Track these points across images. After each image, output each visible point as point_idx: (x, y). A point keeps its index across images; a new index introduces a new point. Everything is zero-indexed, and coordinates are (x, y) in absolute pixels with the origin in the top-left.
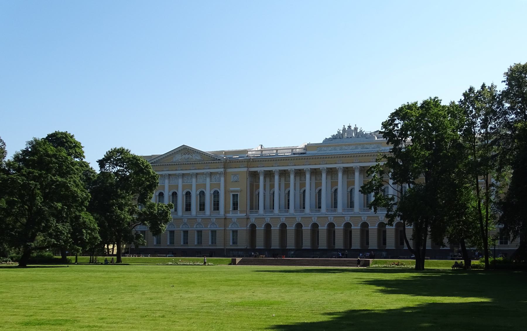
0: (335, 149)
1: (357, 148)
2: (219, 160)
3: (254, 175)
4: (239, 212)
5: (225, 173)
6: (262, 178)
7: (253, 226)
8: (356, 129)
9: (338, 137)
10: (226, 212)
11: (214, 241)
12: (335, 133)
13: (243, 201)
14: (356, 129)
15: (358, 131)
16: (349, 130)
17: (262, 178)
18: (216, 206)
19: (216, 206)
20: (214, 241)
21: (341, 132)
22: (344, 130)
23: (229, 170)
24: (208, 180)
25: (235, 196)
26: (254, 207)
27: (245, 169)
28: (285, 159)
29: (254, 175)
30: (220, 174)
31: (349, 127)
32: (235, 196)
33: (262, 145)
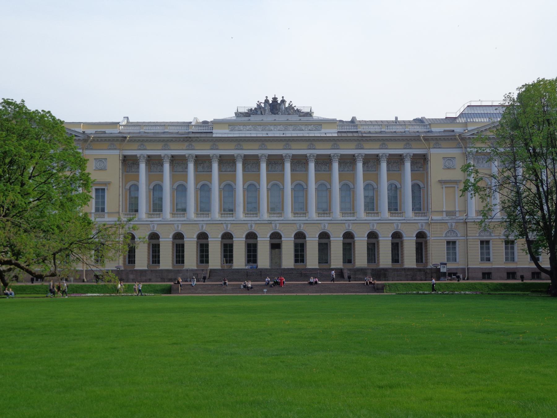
0: (255, 130)
1: (286, 129)
2: (76, 136)
3: (129, 163)
4: (106, 215)
8: (283, 101)
9: (259, 112)
12: (254, 106)
14: (283, 101)
15: (287, 105)
16: (276, 103)
21: (263, 105)
22: (267, 101)
27: (117, 152)
31: (275, 99)
33: (128, 118)
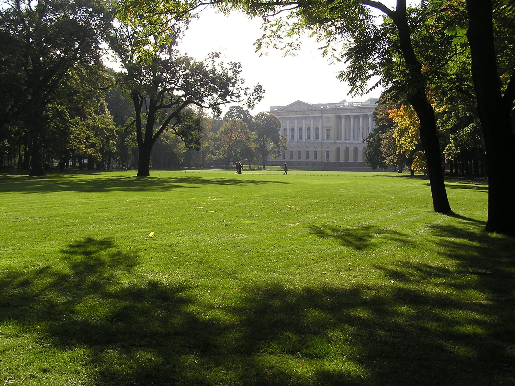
5: (322, 117)
6: (343, 120)
7: (339, 148)
10: (323, 139)
11: (316, 157)
13: (333, 133)
17: (343, 120)
18: (317, 137)
19: (317, 137)
20: (316, 157)
23: (324, 115)
24: (312, 120)
25: (328, 131)
26: (338, 137)
27: (334, 114)
28: (358, 108)
29: (340, 118)
30: (319, 117)
32: (328, 131)
